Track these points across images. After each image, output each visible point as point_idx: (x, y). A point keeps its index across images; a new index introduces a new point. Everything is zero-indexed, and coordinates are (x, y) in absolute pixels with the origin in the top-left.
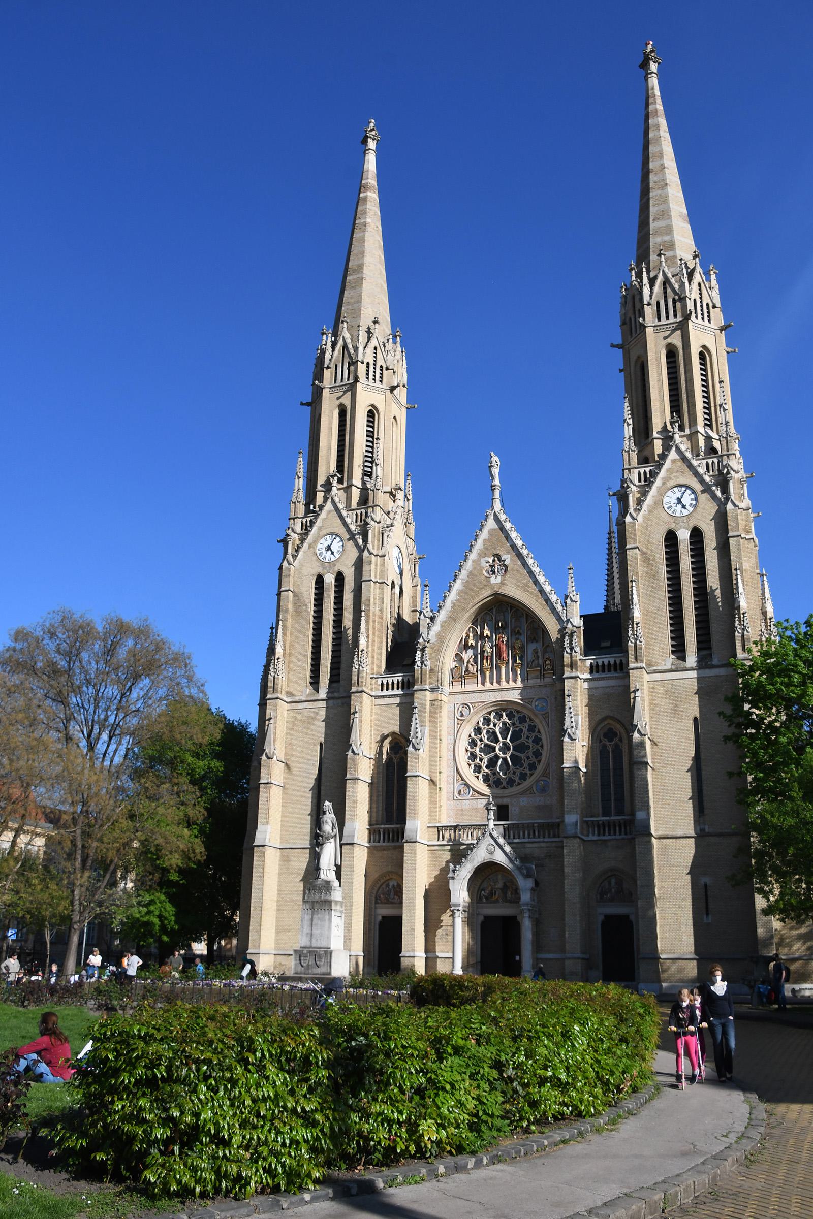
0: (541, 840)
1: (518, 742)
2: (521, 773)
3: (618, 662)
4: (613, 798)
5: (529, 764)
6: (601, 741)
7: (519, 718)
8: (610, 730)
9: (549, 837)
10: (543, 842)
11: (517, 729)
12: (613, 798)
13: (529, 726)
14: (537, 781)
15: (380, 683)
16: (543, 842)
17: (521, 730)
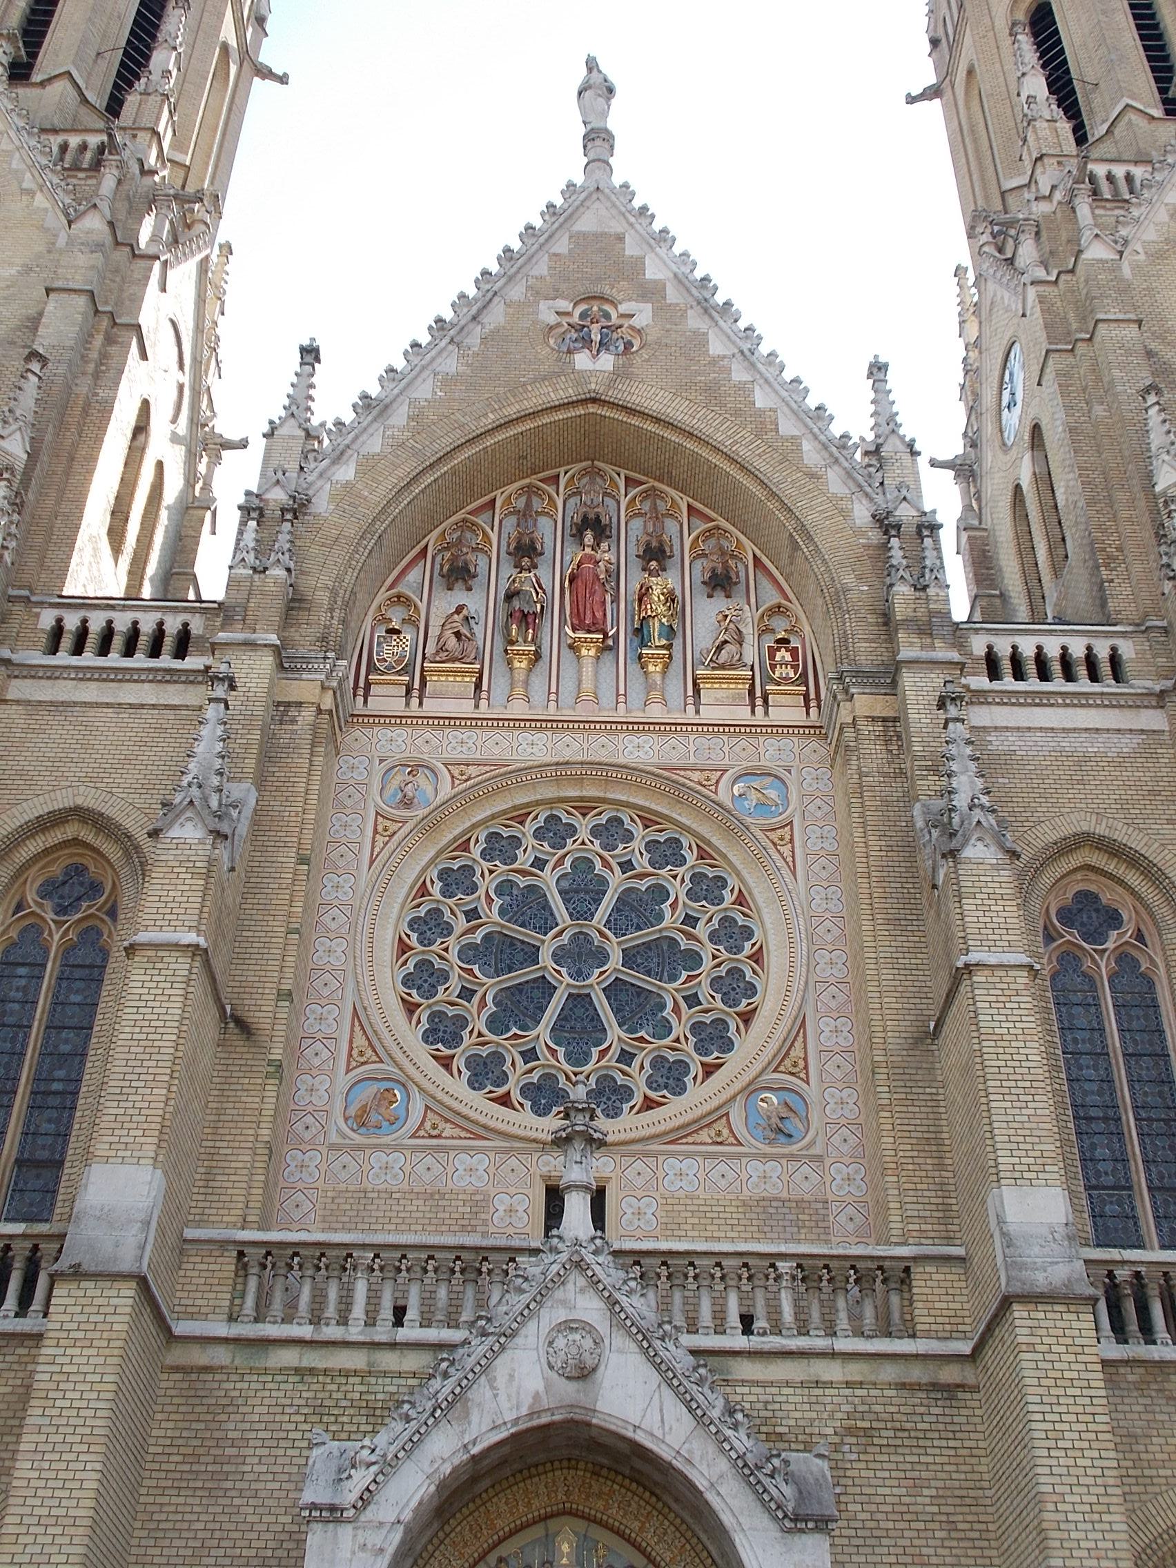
0: (821, 1343)
1: (648, 934)
2: (659, 1062)
3: (1103, 652)
4: (1140, 1178)
5: (697, 1028)
6: (1049, 938)
7: (651, 846)
8: (1088, 899)
9: (859, 1333)
10: (833, 1355)
11: (643, 885)
12: (1140, 1178)
13: (697, 878)
14: (751, 1089)
15: (47, 619)
16: (833, 1355)
17: (660, 893)
